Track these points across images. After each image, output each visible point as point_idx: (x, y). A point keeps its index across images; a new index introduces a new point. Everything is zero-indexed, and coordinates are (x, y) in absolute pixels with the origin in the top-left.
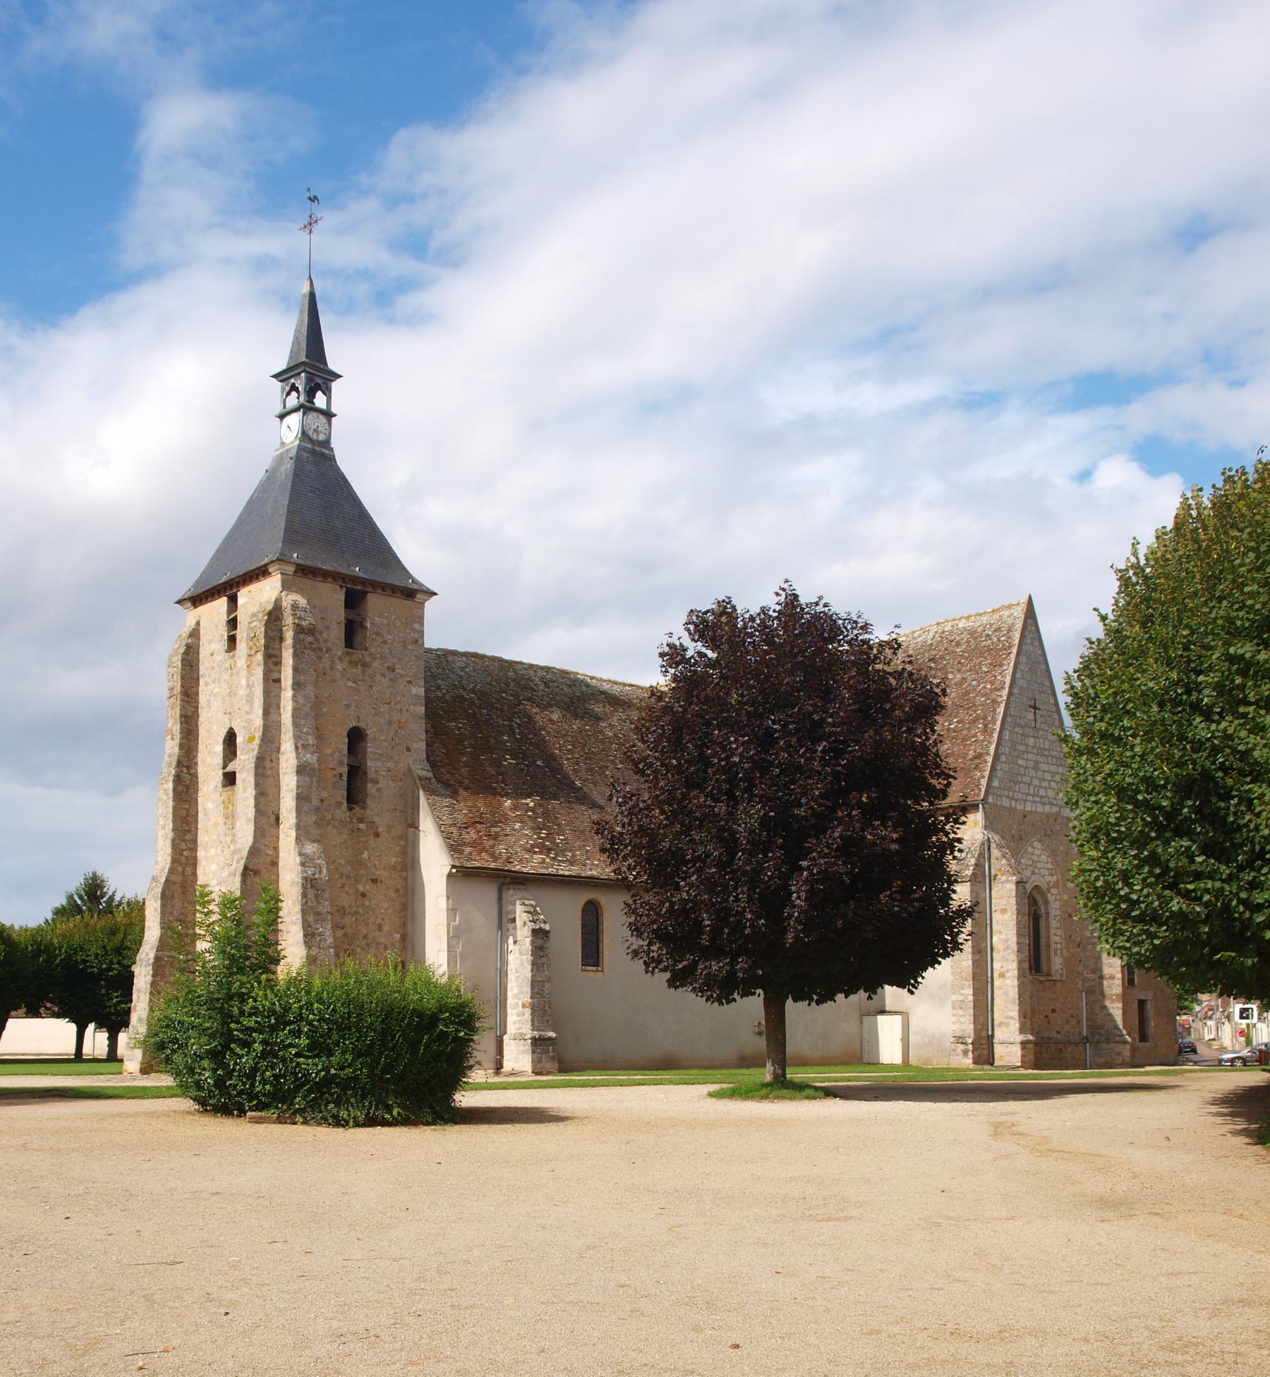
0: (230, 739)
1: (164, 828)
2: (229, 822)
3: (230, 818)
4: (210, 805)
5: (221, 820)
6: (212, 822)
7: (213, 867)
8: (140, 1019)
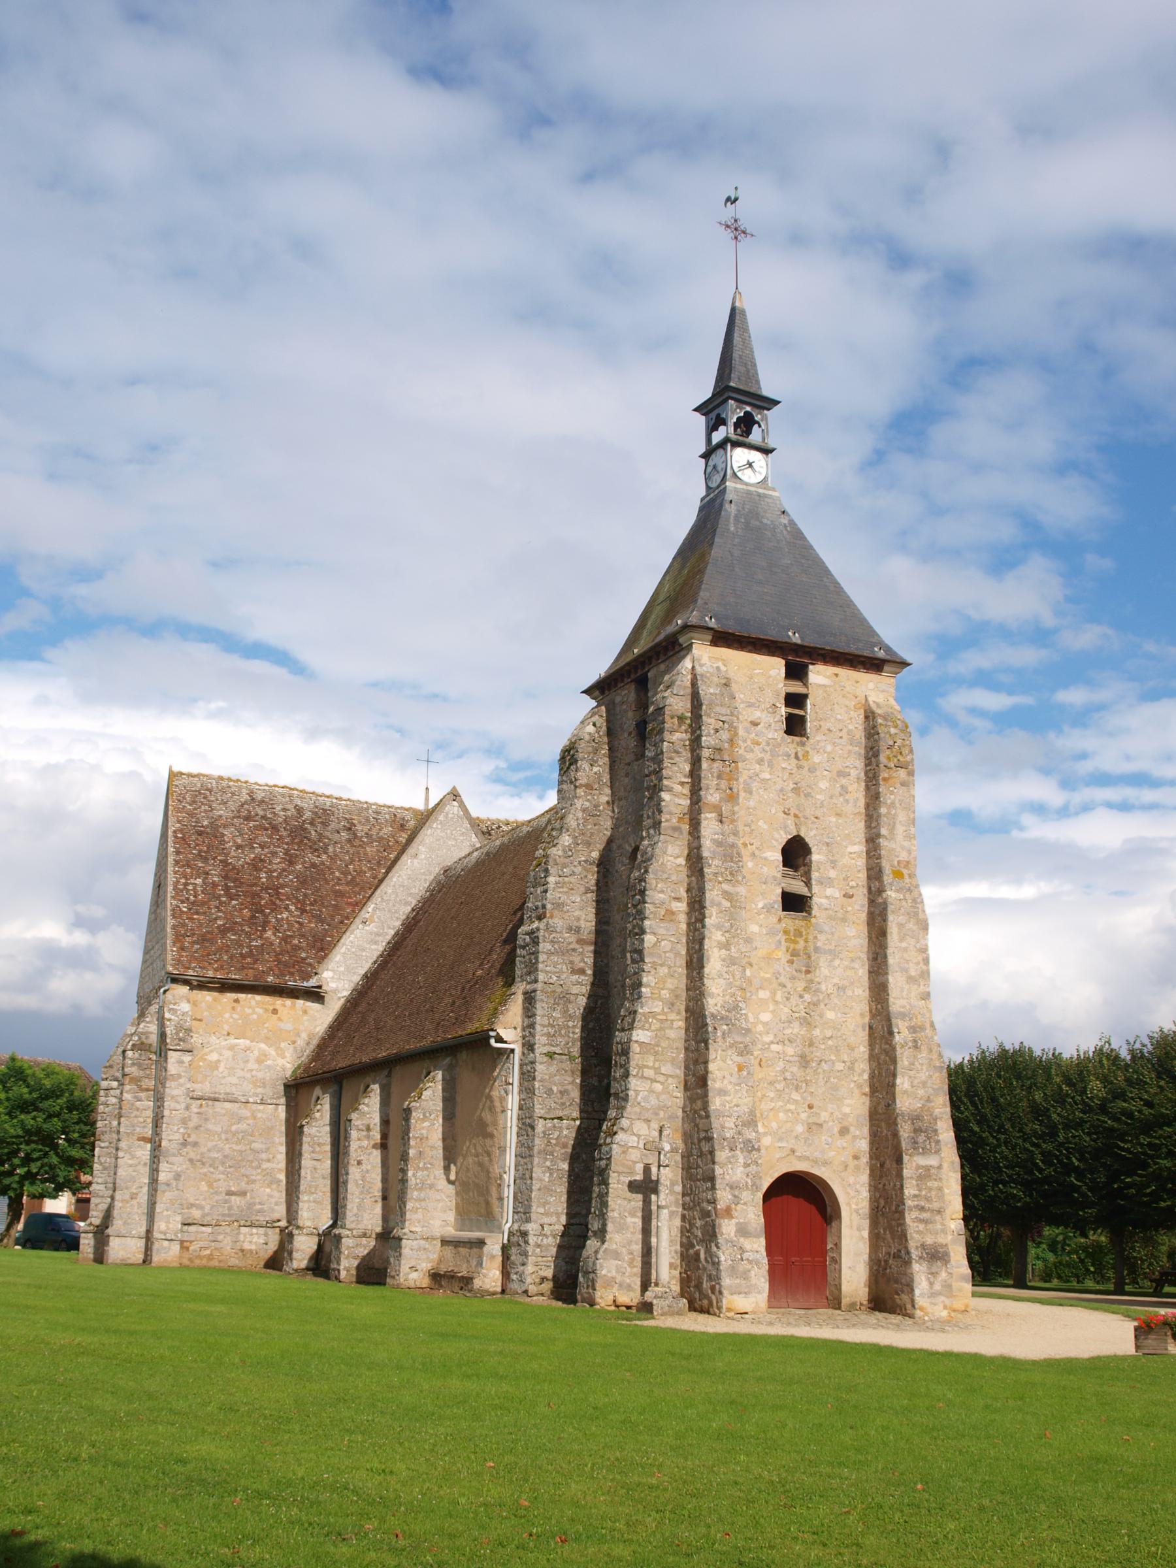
0: (795, 853)
1: (726, 946)
2: (799, 963)
3: (804, 961)
4: (754, 928)
5: (782, 955)
6: (761, 952)
7: (766, 1017)
8: (743, 1231)
